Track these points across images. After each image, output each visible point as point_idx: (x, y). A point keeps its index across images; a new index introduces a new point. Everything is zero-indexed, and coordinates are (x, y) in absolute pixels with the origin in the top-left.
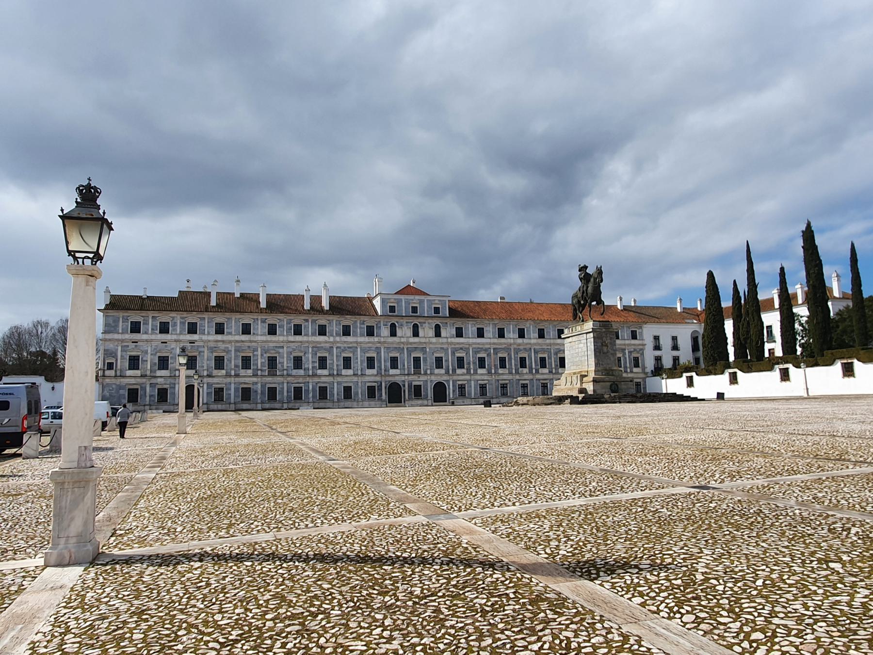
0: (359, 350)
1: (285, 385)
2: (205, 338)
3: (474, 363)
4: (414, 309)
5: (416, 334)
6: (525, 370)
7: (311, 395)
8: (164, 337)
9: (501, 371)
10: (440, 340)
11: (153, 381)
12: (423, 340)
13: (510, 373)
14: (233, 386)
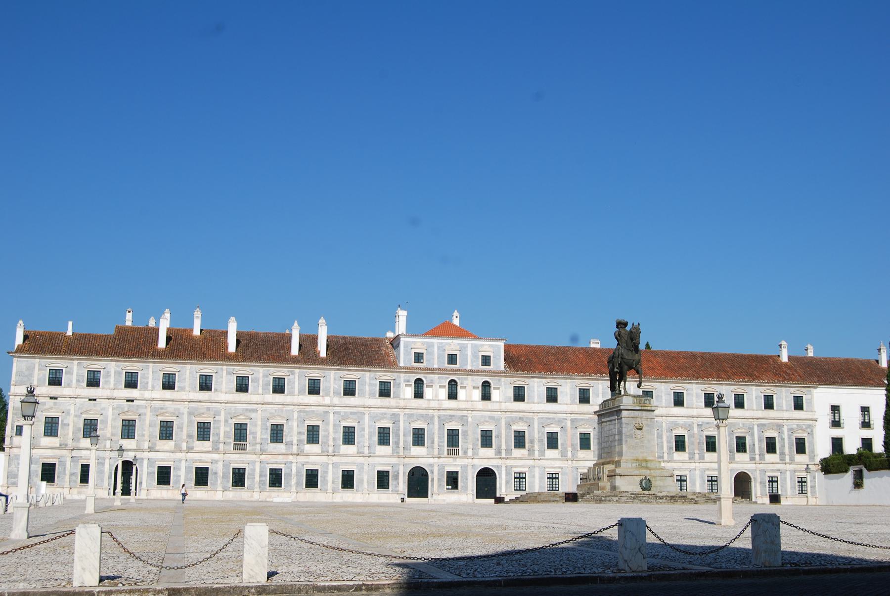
0: (367, 417)
1: (258, 465)
2: (148, 394)
3: (540, 441)
4: (452, 359)
5: (453, 395)
7: (294, 481)
8: (93, 392)
11: (75, 453)
12: (463, 406)
14: (183, 465)
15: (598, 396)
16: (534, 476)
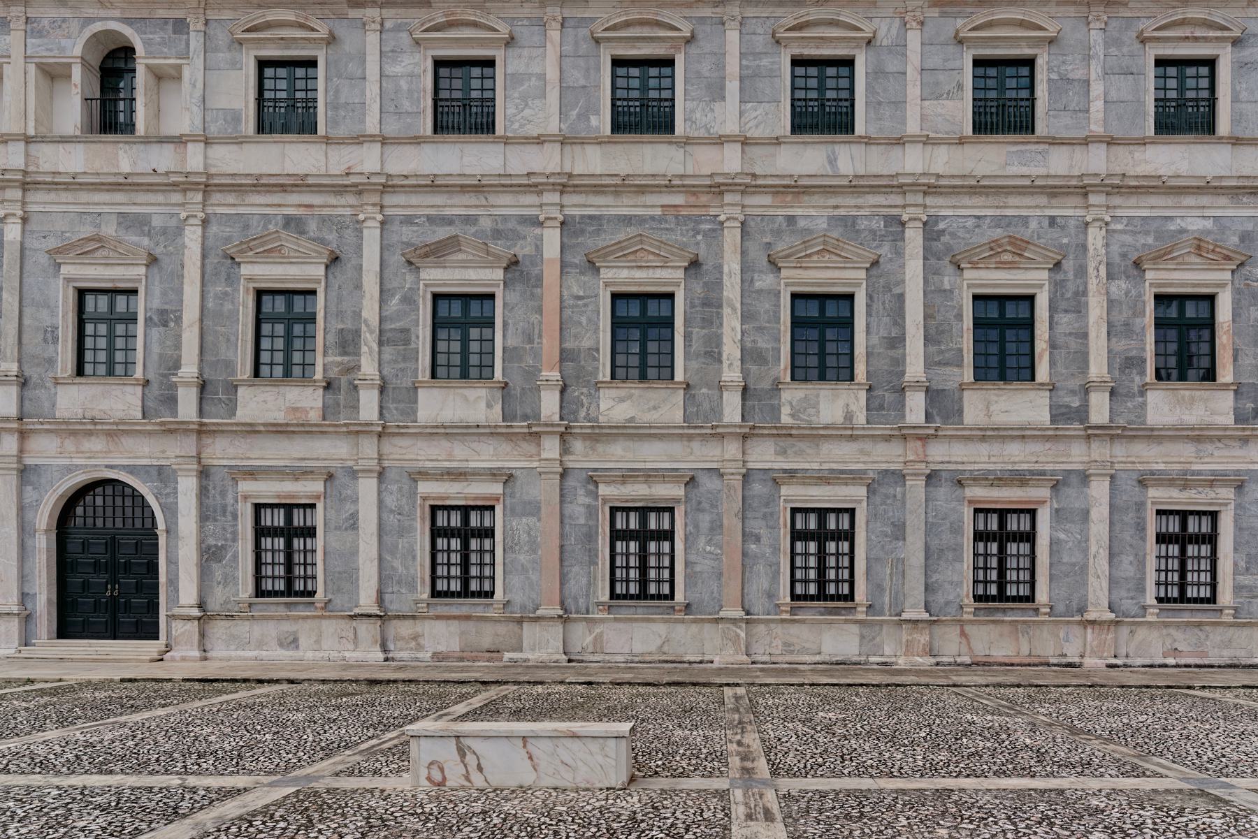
3: (393, 338)
6: (834, 404)
9: (617, 404)
10: (122, 157)
13: (700, 424)
15: (717, 92)
16: (353, 523)
